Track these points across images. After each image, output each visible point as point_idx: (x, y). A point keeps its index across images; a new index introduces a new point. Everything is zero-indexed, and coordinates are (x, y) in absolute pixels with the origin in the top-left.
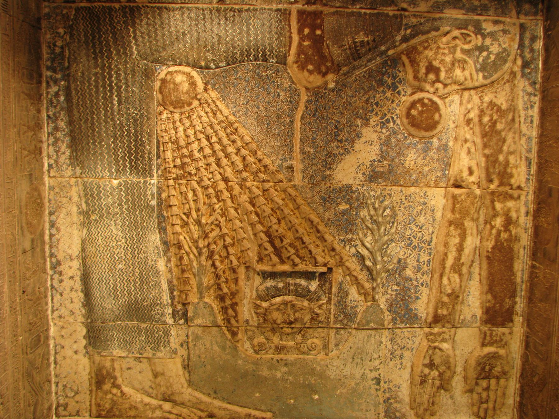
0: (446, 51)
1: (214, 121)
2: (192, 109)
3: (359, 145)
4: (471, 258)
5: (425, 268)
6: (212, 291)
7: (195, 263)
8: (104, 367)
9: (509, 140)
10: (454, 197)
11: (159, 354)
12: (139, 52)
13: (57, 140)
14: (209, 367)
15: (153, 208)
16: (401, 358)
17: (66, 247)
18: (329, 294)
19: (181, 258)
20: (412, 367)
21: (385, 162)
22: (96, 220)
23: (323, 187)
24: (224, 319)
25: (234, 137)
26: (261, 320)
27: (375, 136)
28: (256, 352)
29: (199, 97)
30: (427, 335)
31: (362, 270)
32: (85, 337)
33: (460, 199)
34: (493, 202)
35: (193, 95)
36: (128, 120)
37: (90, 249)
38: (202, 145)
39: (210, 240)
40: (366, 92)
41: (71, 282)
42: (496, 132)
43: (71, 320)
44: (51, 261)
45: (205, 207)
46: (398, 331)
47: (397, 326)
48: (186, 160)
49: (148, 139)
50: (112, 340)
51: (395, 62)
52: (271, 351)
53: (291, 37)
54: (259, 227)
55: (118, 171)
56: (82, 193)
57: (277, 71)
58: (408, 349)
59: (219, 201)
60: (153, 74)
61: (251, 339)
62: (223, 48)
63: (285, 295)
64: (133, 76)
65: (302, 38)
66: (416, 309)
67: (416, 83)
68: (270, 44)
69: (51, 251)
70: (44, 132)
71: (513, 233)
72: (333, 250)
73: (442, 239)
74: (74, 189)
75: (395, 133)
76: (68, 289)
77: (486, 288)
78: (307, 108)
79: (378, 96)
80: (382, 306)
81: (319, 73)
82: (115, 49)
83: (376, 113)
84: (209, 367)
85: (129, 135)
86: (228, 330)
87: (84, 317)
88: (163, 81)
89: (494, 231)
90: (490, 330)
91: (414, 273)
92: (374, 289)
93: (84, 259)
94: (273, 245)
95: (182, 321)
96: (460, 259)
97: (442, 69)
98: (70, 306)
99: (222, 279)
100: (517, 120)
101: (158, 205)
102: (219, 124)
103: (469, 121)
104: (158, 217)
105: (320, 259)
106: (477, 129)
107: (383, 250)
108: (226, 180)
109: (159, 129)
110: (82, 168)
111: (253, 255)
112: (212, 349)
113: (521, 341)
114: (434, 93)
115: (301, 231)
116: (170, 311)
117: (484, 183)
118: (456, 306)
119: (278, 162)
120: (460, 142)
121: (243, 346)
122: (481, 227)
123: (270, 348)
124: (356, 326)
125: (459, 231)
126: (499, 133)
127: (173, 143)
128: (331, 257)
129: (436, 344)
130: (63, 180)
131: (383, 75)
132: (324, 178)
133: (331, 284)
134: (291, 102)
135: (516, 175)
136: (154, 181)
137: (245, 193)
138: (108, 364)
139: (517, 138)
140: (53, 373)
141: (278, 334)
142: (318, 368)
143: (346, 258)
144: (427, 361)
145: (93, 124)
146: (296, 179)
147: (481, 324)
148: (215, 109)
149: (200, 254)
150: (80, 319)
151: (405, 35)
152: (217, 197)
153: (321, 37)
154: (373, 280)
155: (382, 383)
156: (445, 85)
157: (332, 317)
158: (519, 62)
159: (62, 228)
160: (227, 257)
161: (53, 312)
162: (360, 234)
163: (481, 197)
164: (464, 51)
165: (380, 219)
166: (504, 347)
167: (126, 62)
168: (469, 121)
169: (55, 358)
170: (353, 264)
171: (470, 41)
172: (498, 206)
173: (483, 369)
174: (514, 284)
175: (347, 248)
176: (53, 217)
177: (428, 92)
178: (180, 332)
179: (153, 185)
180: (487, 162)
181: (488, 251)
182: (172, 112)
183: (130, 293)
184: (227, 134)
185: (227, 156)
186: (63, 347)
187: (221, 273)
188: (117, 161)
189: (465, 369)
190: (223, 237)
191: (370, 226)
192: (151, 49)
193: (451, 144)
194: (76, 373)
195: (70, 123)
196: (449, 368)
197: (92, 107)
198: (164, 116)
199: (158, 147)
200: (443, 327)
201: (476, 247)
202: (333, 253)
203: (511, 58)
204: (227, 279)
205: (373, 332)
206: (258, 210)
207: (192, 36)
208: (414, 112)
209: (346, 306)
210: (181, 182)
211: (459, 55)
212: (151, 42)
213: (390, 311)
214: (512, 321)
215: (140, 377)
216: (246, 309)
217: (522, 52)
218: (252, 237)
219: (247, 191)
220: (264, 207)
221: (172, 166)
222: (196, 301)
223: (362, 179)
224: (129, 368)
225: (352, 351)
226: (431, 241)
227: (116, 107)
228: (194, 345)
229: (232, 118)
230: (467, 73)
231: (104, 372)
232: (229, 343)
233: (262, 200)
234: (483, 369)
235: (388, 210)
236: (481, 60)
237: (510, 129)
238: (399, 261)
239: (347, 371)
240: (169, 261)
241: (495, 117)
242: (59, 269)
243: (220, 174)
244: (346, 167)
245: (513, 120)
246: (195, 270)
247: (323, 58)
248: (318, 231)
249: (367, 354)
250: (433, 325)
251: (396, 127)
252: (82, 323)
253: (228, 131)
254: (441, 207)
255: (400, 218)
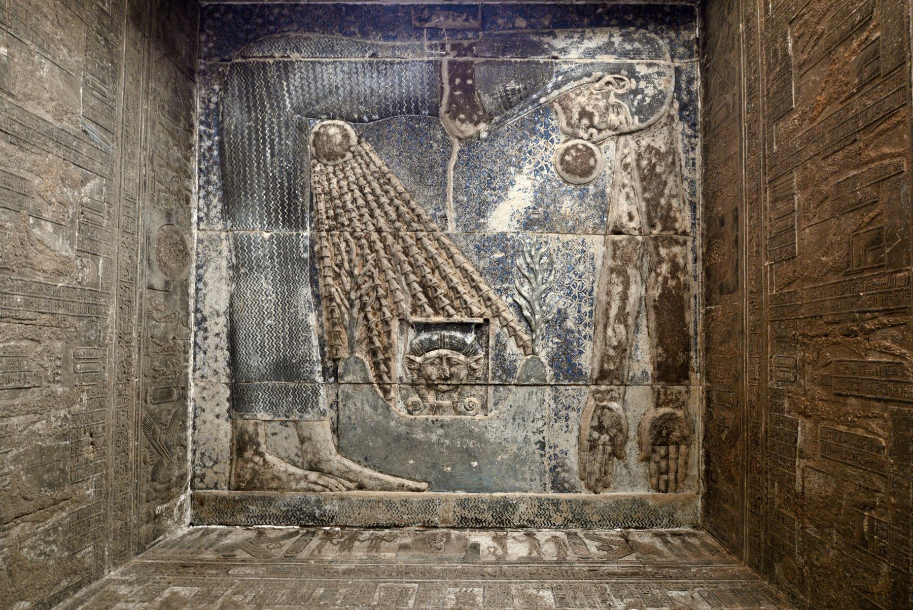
0: (599, 97)
1: (367, 172)
2: (345, 162)
3: (513, 192)
4: (636, 308)
5: (587, 319)
6: (364, 346)
7: (346, 316)
8: (246, 431)
9: (670, 183)
10: (614, 243)
11: (307, 416)
12: (292, 105)
13: (208, 193)
14: (359, 430)
15: (305, 261)
16: (567, 420)
17: (213, 302)
18: (487, 347)
19: (332, 311)
20: (579, 430)
21: (540, 209)
22: (245, 274)
23: (478, 235)
24: (375, 376)
25: (387, 187)
26: (416, 376)
27: (528, 184)
28: (410, 413)
29: (352, 149)
30: (594, 393)
31: (520, 321)
32: (228, 400)
33: (620, 245)
34: (656, 247)
35: (346, 147)
36: (281, 172)
37: (238, 304)
38: (355, 196)
39: (363, 291)
40: (519, 141)
41: (217, 339)
42: (656, 175)
43: (214, 380)
44: (196, 317)
45: (358, 258)
46: (562, 388)
47: (560, 383)
48: (339, 211)
49: (301, 192)
50: (256, 401)
51: (547, 110)
52: (426, 411)
53: (442, 88)
54: (412, 277)
55: (269, 223)
56: (232, 246)
57: (430, 123)
58: (573, 409)
59: (372, 252)
60: (307, 127)
61: (404, 398)
62: (375, 100)
63: (440, 348)
64: (287, 129)
65: (454, 88)
66: (580, 364)
67: (569, 130)
68: (422, 95)
69: (196, 306)
70: (194, 183)
71: (682, 279)
72: (489, 299)
73: (604, 287)
74: (225, 243)
75: (549, 180)
76: (213, 347)
77: (656, 340)
78: (459, 157)
79: (531, 144)
80: (543, 360)
81: (471, 122)
82: (269, 103)
83: (530, 162)
84: (359, 430)
85: (282, 188)
86: (380, 388)
87: (229, 377)
88: (317, 134)
89: (660, 279)
90: (663, 388)
91: (575, 324)
92: (533, 341)
93: (231, 315)
94: (427, 296)
95: (332, 379)
96: (625, 308)
97: (596, 113)
98: (214, 366)
99: (375, 332)
100: (677, 163)
101: (310, 258)
102: (372, 175)
103: (626, 166)
104: (310, 270)
105: (475, 310)
106: (636, 174)
107: (541, 299)
108: (379, 231)
109: (312, 182)
110: (233, 221)
111: (406, 307)
112: (363, 409)
113: (701, 400)
114: (589, 139)
115: (455, 280)
116: (320, 369)
117: (646, 229)
118: (624, 361)
119: (431, 211)
120: (617, 188)
121: (395, 405)
122: (645, 276)
123: (425, 407)
124: (516, 382)
125: (621, 279)
126: (659, 176)
127: (325, 194)
128: (487, 307)
129: (605, 403)
130: (214, 233)
131: (536, 123)
132: (478, 226)
133: (488, 337)
134: (443, 152)
135: (680, 220)
136: (307, 233)
137: (398, 243)
138: (251, 429)
139: (678, 182)
140: (190, 439)
141: (433, 393)
142: (477, 430)
143: (502, 308)
144: (595, 423)
145: (245, 176)
146: (450, 228)
147: (654, 381)
148: (368, 160)
149: (352, 306)
150: (225, 379)
151: (556, 82)
152: (370, 248)
153: (472, 87)
154: (532, 331)
155: (547, 448)
156: (600, 131)
157: (490, 372)
158: (676, 105)
159: (210, 282)
160: (380, 309)
161: (194, 371)
162: (517, 283)
163: (643, 243)
164: (617, 95)
165: (537, 267)
166: (681, 408)
167: (279, 115)
168: (626, 166)
169: (194, 423)
170: (510, 315)
171: (624, 86)
172: (663, 252)
173: (660, 433)
174: (687, 336)
175: (504, 297)
176: (201, 271)
177: (582, 138)
178: (330, 392)
179: (306, 237)
180: (648, 206)
181: (655, 301)
182: (325, 165)
183: (278, 350)
184: (380, 185)
185: (380, 206)
186: (204, 410)
187: (373, 326)
188: (269, 214)
189: (639, 434)
190: (375, 288)
191: (527, 274)
192: (304, 102)
193: (608, 190)
194: (216, 440)
195: (223, 177)
196: (620, 430)
197: (245, 159)
198: (318, 169)
199: (311, 200)
200: (611, 384)
201: (641, 298)
202: (489, 303)
203: (668, 101)
204: (379, 332)
205: (535, 389)
206: (411, 259)
207: (345, 89)
208: (568, 158)
209: (505, 360)
210: (333, 232)
211: (612, 99)
212: (304, 95)
213: (551, 366)
214: (688, 378)
215: (285, 444)
216: (399, 365)
217: (679, 94)
218: (406, 288)
219: (400, 240)
220: (417, 256)
221: (324, 217)
222: (347, 356)
223: (517, 226)
224: (274, 434)
225: (513, 410)
226: (592, 290)
227: (269, 159)
228: (344, 405)
229: (385, 169)
230: (622, 117)
231: (247, 437)
232: (381, 402)
233: (415, 249)
234: (660, 433)
235: (545, 258)
236: (636, 103)
237: (671, 172)
238: (559, 311)
239: (508, 434)
240: (320, 315)
241: (654, 160)
242: (204, 325)
243: (374, 224)
244: (499, 215)
245: (673, 163)
246: (346, 323)
247: (474, 107)
248: (473, 280)
249: (529, 413)
250: (599, 382)
251: (550, 175)
252: (226, 384)
253: (381, 181)
254: (601, 256)
255: (558, 266)
